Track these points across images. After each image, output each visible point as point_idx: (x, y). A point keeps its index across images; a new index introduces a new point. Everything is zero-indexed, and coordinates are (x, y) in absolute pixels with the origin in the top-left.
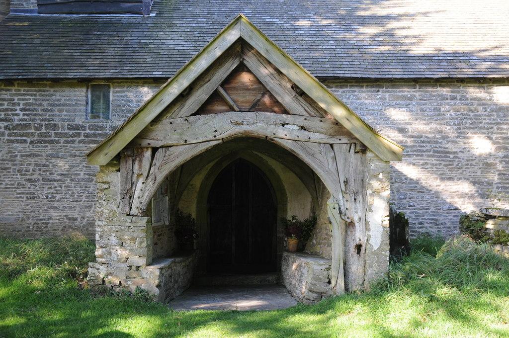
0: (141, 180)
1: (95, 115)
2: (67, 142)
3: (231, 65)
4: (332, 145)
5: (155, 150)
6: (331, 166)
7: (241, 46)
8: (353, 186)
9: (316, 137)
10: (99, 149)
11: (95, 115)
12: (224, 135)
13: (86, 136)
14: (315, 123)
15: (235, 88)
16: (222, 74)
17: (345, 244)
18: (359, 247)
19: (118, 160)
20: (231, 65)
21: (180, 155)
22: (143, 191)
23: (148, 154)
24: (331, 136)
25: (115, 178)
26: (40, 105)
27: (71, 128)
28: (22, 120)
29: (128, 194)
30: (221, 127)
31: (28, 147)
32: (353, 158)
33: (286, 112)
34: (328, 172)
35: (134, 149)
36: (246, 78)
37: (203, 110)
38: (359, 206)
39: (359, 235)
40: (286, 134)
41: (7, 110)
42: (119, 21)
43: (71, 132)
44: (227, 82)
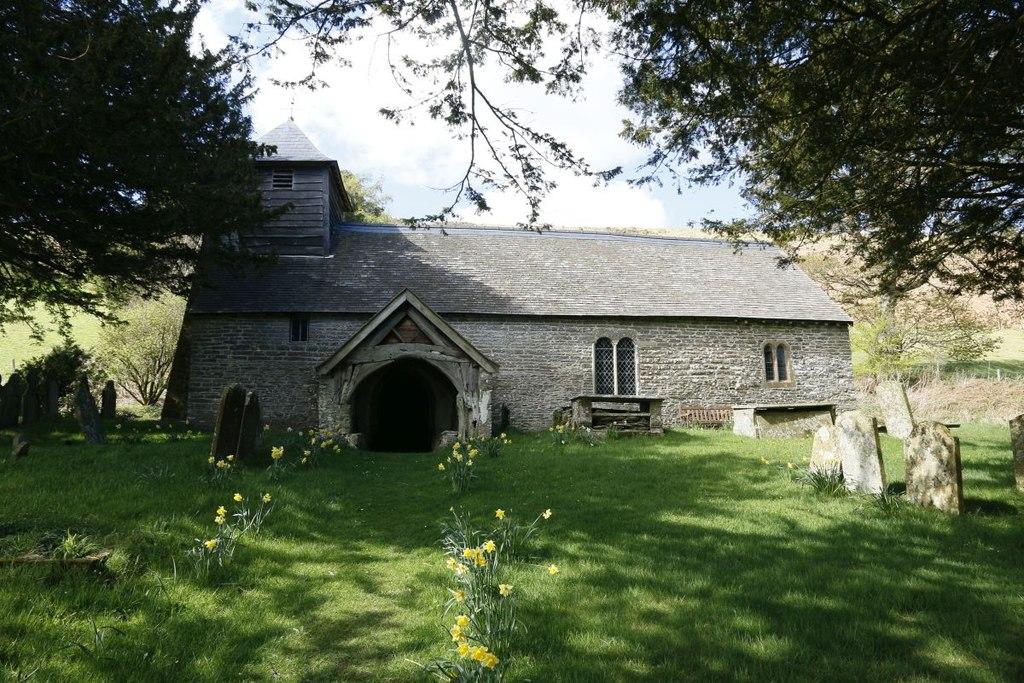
0: (346, 384)
1: (296, 338)
2: (275, 359)
3: (401, 317)
4: (459, 364)
5: (354, 366)
6: (459, 376)
7: (407, 305)
8: (471, 387)
9: (451, 358)
10: (323, 365)
11: (296, 338)
12: (397, 356)
13: (290, 354)
14: (450, 350)
15: (403, 330)
16: (395, 322)
17: (467, 422)
18: (475, 423)
19: (332, 373)
20: (401, 317)
21: (370, 368)
22: (348, 389)
23: (350, 368)
24: (459, 357)
25: (332, 384)
26: (257, 331)
27: (279, 348)
28: (243, 342)
29: (339, 391)
30: (392, 351)
31: (248, 362)
32: (471, 370)
33: (432, 343)
34: (457, 379)
35: (343, 365)
36: (408, 323)
37: (384, 342)
38: (475, 399)
39: (474, 415)
40: (434, 354)
41: (232, 335)
42: (304, 260)
43: (279, 352)
44: (397, 326)
